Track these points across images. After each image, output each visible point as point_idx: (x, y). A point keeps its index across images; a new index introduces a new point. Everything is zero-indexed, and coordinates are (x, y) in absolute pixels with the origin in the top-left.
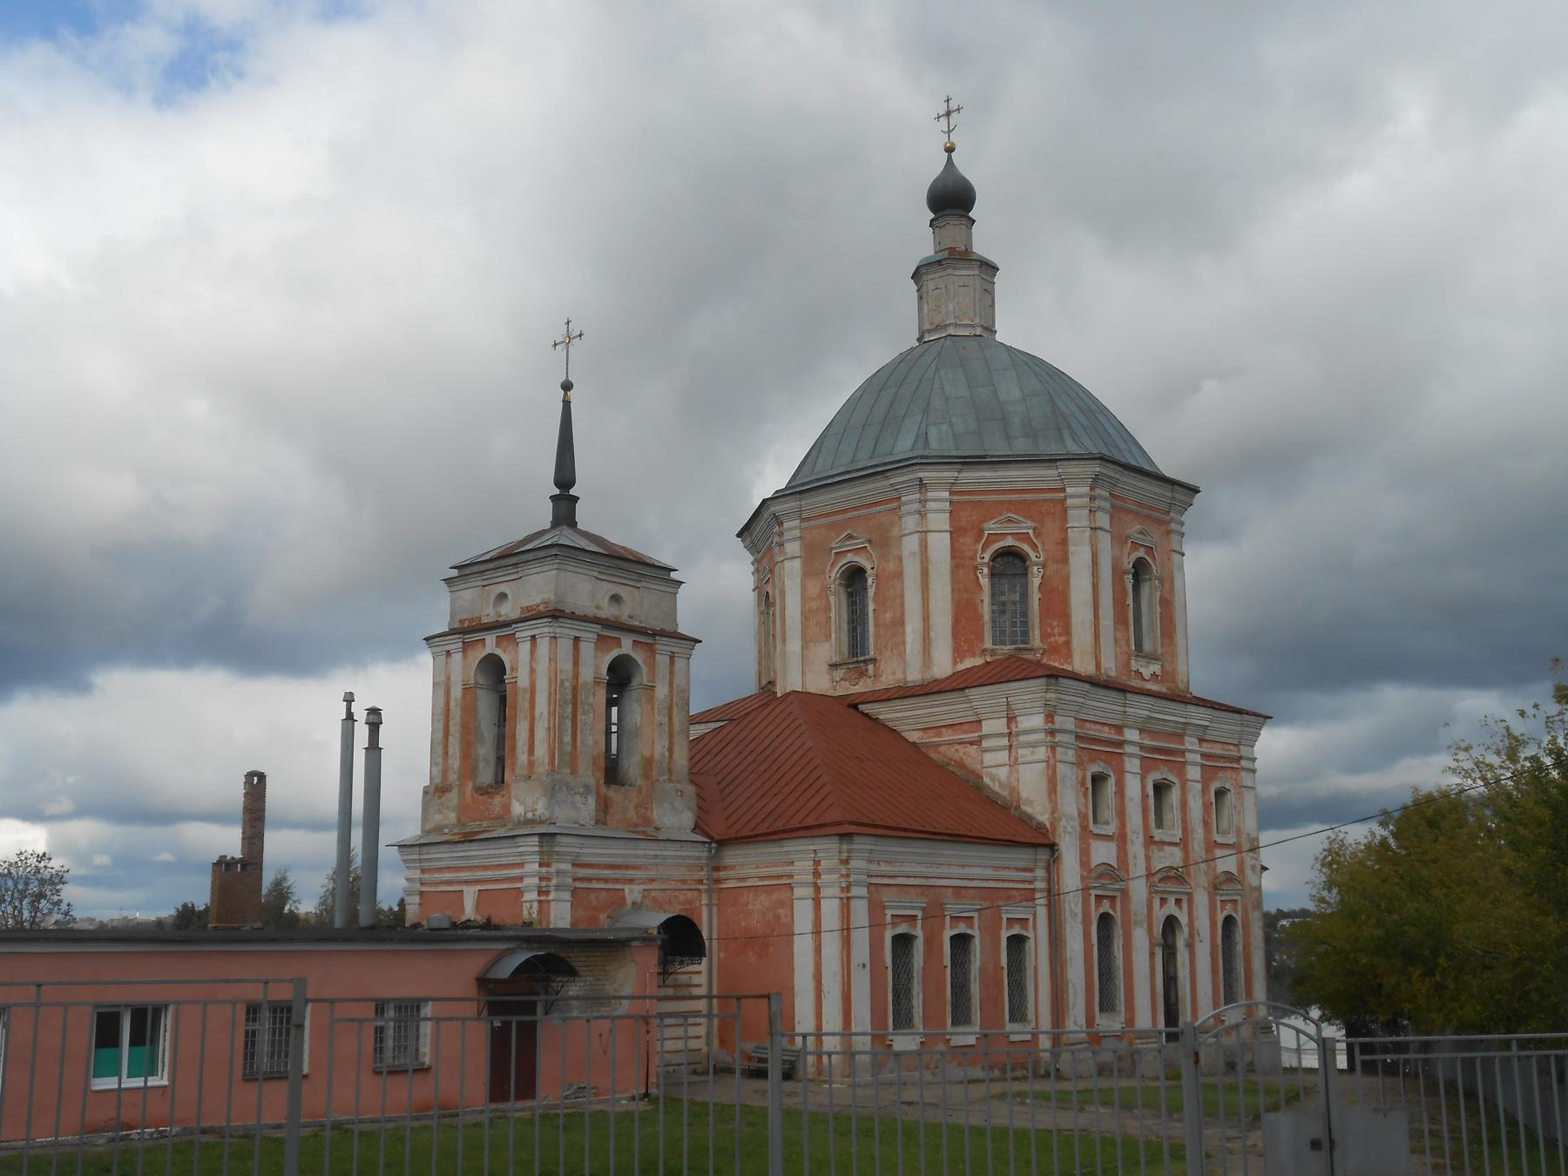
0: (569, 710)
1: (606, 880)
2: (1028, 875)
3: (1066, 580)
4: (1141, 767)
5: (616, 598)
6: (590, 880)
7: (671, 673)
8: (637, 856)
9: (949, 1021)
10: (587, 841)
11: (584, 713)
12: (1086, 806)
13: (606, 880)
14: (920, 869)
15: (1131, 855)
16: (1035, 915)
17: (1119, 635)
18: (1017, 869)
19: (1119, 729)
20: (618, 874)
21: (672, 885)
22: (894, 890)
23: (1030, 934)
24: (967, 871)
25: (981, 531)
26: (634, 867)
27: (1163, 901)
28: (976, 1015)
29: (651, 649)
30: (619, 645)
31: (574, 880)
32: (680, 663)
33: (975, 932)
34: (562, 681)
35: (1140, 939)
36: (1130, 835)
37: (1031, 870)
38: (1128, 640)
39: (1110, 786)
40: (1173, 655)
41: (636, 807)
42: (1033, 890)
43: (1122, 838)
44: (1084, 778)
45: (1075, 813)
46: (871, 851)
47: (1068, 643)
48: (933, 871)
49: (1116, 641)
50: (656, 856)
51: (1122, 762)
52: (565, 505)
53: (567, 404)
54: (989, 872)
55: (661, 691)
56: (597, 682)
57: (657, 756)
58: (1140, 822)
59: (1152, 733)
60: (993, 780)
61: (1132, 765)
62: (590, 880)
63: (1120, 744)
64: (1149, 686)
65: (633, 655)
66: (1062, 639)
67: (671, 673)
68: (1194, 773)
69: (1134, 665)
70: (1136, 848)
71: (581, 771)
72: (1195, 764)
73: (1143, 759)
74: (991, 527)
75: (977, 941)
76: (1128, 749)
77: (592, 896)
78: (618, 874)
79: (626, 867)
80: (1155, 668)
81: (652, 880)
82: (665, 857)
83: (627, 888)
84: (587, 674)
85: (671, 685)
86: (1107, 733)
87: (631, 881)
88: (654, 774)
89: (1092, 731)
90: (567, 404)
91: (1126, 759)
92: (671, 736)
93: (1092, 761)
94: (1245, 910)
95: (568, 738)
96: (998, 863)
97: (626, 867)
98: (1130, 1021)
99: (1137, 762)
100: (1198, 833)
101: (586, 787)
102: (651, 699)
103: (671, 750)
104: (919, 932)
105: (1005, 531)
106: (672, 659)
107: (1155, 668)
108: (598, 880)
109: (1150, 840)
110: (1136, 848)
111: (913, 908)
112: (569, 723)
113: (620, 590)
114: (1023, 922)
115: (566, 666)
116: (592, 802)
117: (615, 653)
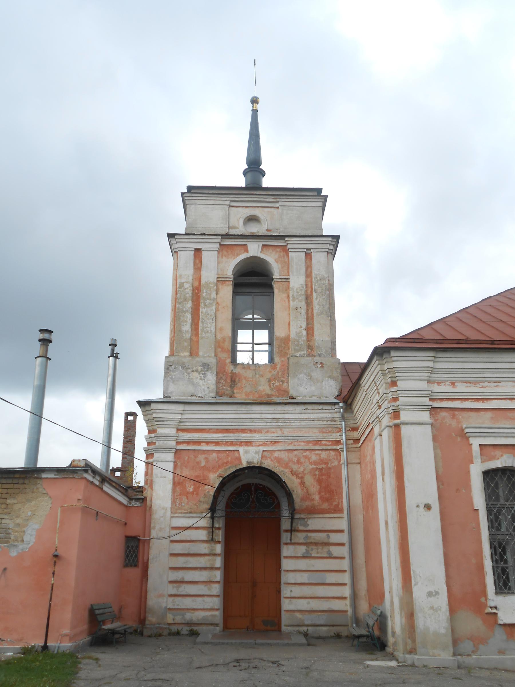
0: (189, 305)
1: (217, 443)
6: (199, 443)
8: (252, 420)
10: (188, 408)
13: (217, 443)
20: (231, 437)
21: (303, 446)
26: (251, 431)
30: (247, 251)
31: (178, 443)
34: (182, 284)
41: (270, 381)
50: (277, 420)
56: (220, 281)
62: (199, 443)
65: (263, 256)
71: (201, 353)
77: (201, 458)
78: (231, 437)
79: (243, 431)
82: (285, 420)
83: (241, 449)
84: (209, 275)
87: (248, 443)
88: (291, 351)
92: (310, 319)
95: (187, 327)
97: (243, 431)
101: (204, 365)
103: (310, 329)
108: (207, 443)
112: (189, 316)
113: (257, 212)
115: (188, 272)
116: (211, 378)
117: (243, 256)
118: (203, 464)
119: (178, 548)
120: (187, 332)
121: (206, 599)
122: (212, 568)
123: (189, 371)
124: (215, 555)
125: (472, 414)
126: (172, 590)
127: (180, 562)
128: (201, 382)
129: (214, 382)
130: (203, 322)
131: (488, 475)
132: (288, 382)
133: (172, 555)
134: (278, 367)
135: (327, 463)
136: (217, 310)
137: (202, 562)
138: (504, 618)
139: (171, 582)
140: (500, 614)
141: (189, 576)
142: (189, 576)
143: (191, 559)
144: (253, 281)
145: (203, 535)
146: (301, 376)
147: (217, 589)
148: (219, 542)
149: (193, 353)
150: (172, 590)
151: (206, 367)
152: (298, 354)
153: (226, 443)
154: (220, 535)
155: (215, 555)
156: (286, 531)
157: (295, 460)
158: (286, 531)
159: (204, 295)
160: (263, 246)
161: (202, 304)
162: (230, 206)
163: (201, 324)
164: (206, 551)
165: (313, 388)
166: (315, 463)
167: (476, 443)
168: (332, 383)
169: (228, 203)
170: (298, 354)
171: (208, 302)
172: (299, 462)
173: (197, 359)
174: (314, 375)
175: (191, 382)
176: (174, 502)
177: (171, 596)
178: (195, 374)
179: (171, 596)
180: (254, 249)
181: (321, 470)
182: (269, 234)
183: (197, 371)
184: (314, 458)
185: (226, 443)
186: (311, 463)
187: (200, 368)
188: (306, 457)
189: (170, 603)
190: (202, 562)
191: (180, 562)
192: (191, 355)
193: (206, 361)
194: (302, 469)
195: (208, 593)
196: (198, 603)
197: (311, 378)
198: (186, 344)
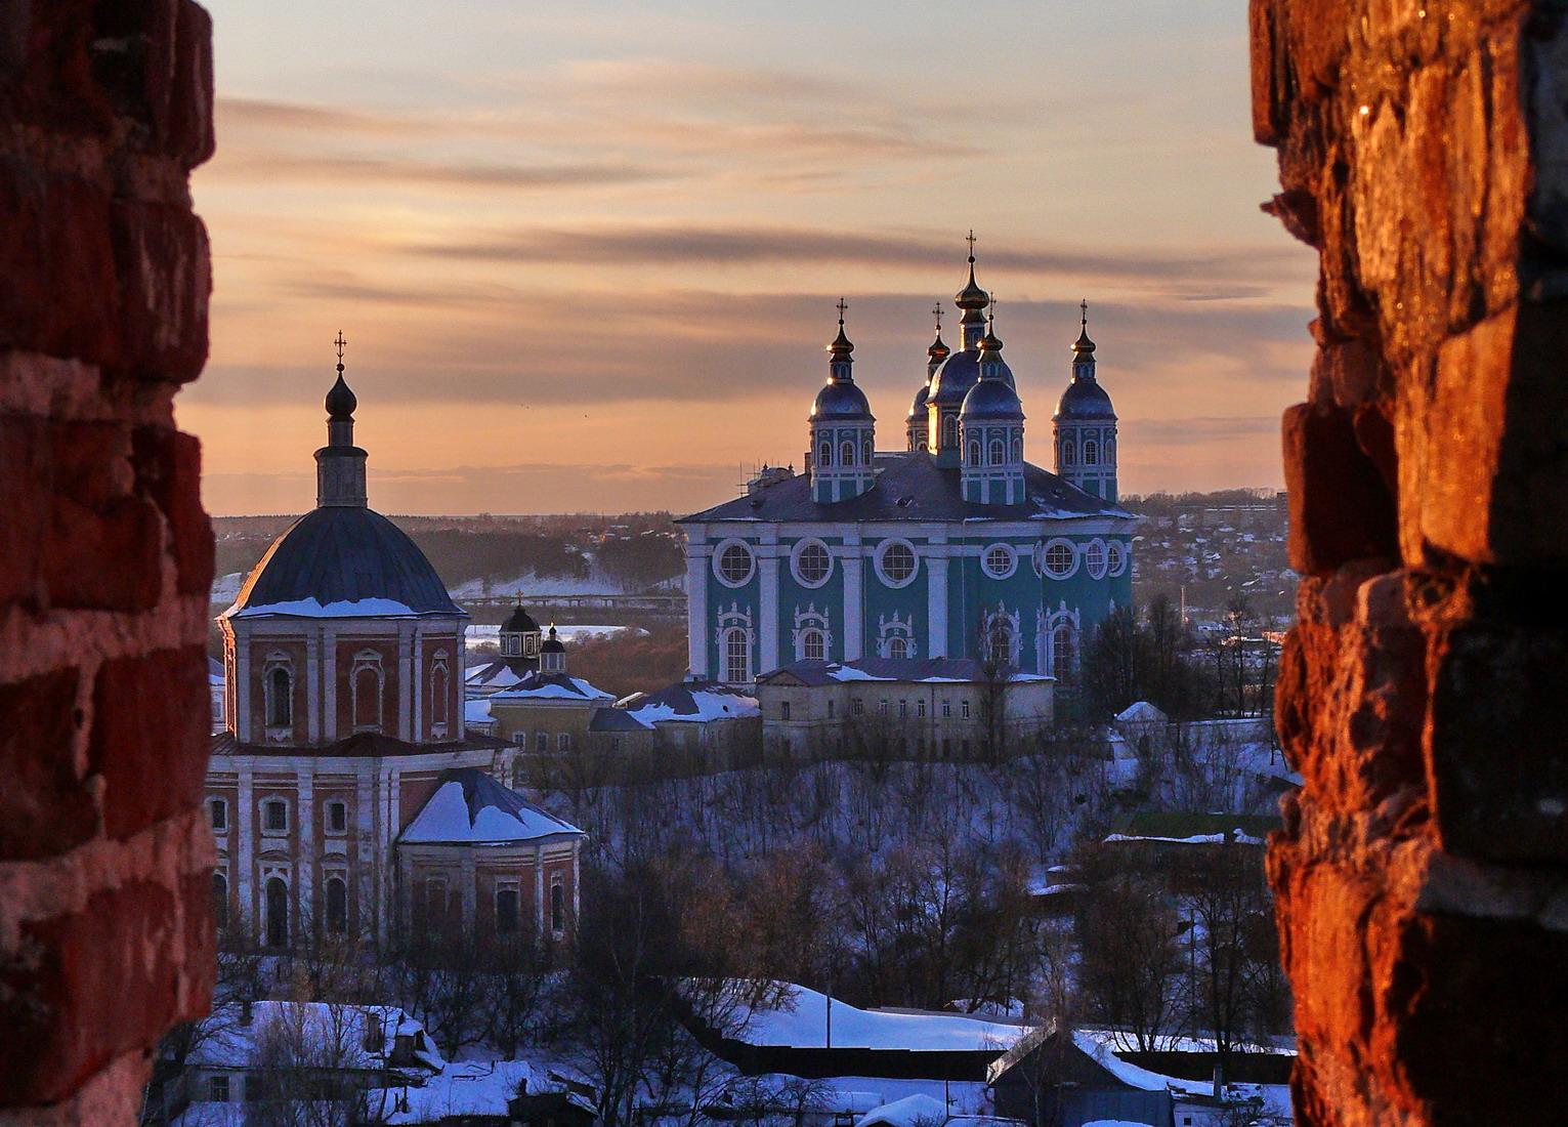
17: (257, 718)
19: (236, 775)
27: (267, 870)
43: (234, 837)
68: (306, 794)
70: (246, 840)
109: (258, 836)
110: (246, 840)
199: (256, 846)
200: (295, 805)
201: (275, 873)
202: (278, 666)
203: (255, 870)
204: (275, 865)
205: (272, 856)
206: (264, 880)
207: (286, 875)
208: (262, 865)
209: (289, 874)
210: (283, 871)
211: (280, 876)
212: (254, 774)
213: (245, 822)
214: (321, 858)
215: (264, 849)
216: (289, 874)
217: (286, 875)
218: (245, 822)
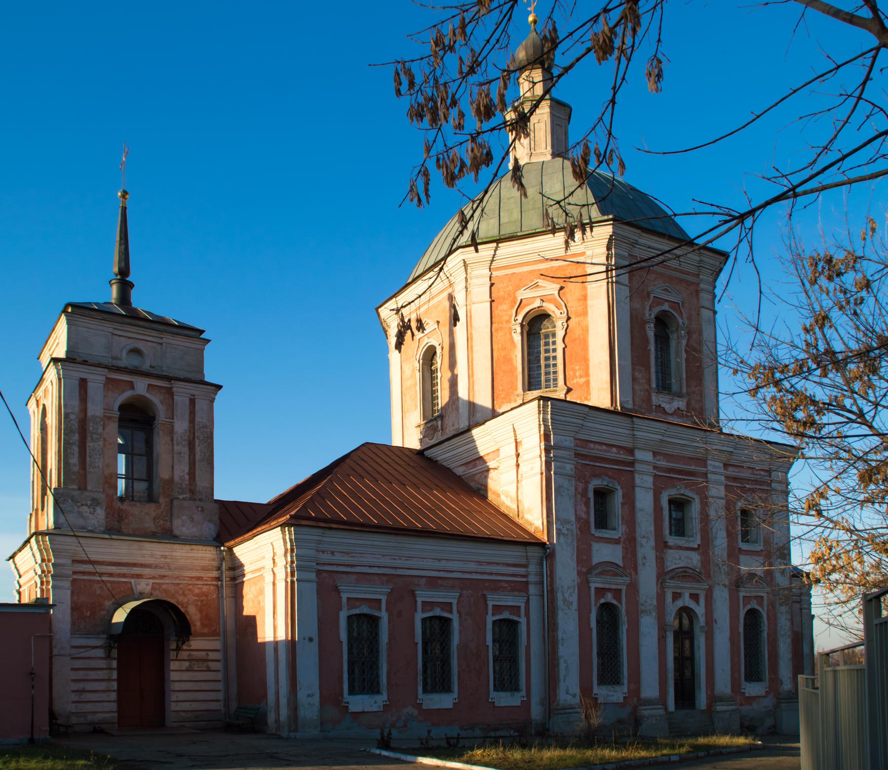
2: (521, 571)
3: (586, 330)
4: (654, 484)
5: (136, 351)
7: (192, 413)
9: (420, 689)
11: (93, 440)
12: (588, 513)
14: (387, 561)
15: (640, 555)
16: (527, 602)
18: (508, 565)
19: (631, 451)
22: (354, 577)
23: (523, 620)
24: (443, 563)
25: (515, 298)
27: (676, 596)
28: (455, 687)
29: (170, 392)
32: (200, 404)
33: (455, 617)
35: (648, 625)
36: (639, 539)
37: (525, 566)
38: (649, 381)
39: (618, 498)
40: (701, 395)
42: (527, 583)
43: (630, 543)
44: (586, 490)
45: (573, 519)
46: (319, 542)
47: (587, 383)
48: (398, 563)
49: (634, 379)
51: (633, 478)
52: (125, 287)
53: (124, 209)
54: (472, 566)
55: (181, 426)
57: (176, 479)
58: (652, 528)
59: (668, 457)
60: (507, 496)
61: (644, 481)
63: (632, 464)
64: (671, 419)
66: (583, 380)
67: (192, 413)
69: (656, 399)
70: (647, 550)
72: (717, 483)
73: (655, 476)
74: (522, 294)
75: (456, 625)
76: (638, 467)
80: (680, 404)
81: (163, 577)
85: (192, 421)
86: (613, 454)
89: (597, 451)
90: (124, 209)
91: (637, 476)
93: (595, 476)
94: (772, 605)
96: (483, 559)
98: (635, 690)
99: (650, 479)
100: (721, 541)
101: (93, 500)
102: (171, 432)
104: (384, 615)
105: (535, 296)
106: (192, 402)
107: (680, 404)
109: (662, 546)
110: (647, 550)
111: (381, 593)
114: (515, 609)
116: (101, 513)
118: (98, 592)
119: (79, 664)
120: (75, 465)
121: (105, 704)
122: (109, 680)
123: (79, 504)
124: (112, 669)
125: (344, 576)
126: (74, 697)
127: (81, 675)
128: (91, 516)
129: (103, 517)
130: (90, 457)
131: (349, 617)
132: (171, 521)
133: (73, 669)
134: (163, 506)
135: (207, 596)
136: (104, 446)
137: (101, 675)
138: (353, 708)
139: (73, 691)
140: (350, 706)
141: (89, 686)
142: (89, 686)
143: (91, 673)
144: (137, 419)
145: (100, 653)
146: (184, 517)
147: (114, 696)
148: (115, 659)
149: (83, 488)
150: (74, 697)
151: (95, 502)
152: (181, 497)
153: (119, 575)
154: (115, 653)
155: (112, 669)
156: (174, 650)
157: (181, 592)
158: (174, 650)
159: (91, 428)
160: (149, 385)
161: (89, 438)
162: (113, 334)
163: (88, 459)
164: (104, 666)
165: (195, 530)
166: (197, 595)
167: (344, 596)
168: (212, 526)
169: (111, 330)
170: (181, 497)
171: (95, 436)
172: (184, 595)
173: (87, 493)
174: (195, 517)
175: (80, 514)
176: (73, 623)
177: (73, 702)
178: (85, 508)
179: (73, 702)
180: (141, 386)
181: (202, 601)
182: (154, 371)
183: (86, 505)
184: (196, 591)
185: (119, 575)
186: (194, 595)
187: (89, 502)
188: (190, 590)
189: (72, 708)
190: (101, 675)
191: (81, 675)
192: (79, 489)
193: (95, 495)
194: (186, 600)
195: (107, 699)
196: (99, 707)
197: (192, 519)
198: (74, 477)
199: (660, 561)
200: (705, 504)
201: (686, 601)
202: (666, 307)
203: (661, 598)
204: (687, 589)
205: (685, 574)
206: (672, 608)
207: (697, 602)
208: (672, 585)
209: (702, 601)
210: (695, 597)
211: (692, 604)
212: (655, 454)
213: (645, 525)
214: (738, 583)
215: (670, 565)
216: (702, 601)
217: (697, 602)
218: (645, 525)
